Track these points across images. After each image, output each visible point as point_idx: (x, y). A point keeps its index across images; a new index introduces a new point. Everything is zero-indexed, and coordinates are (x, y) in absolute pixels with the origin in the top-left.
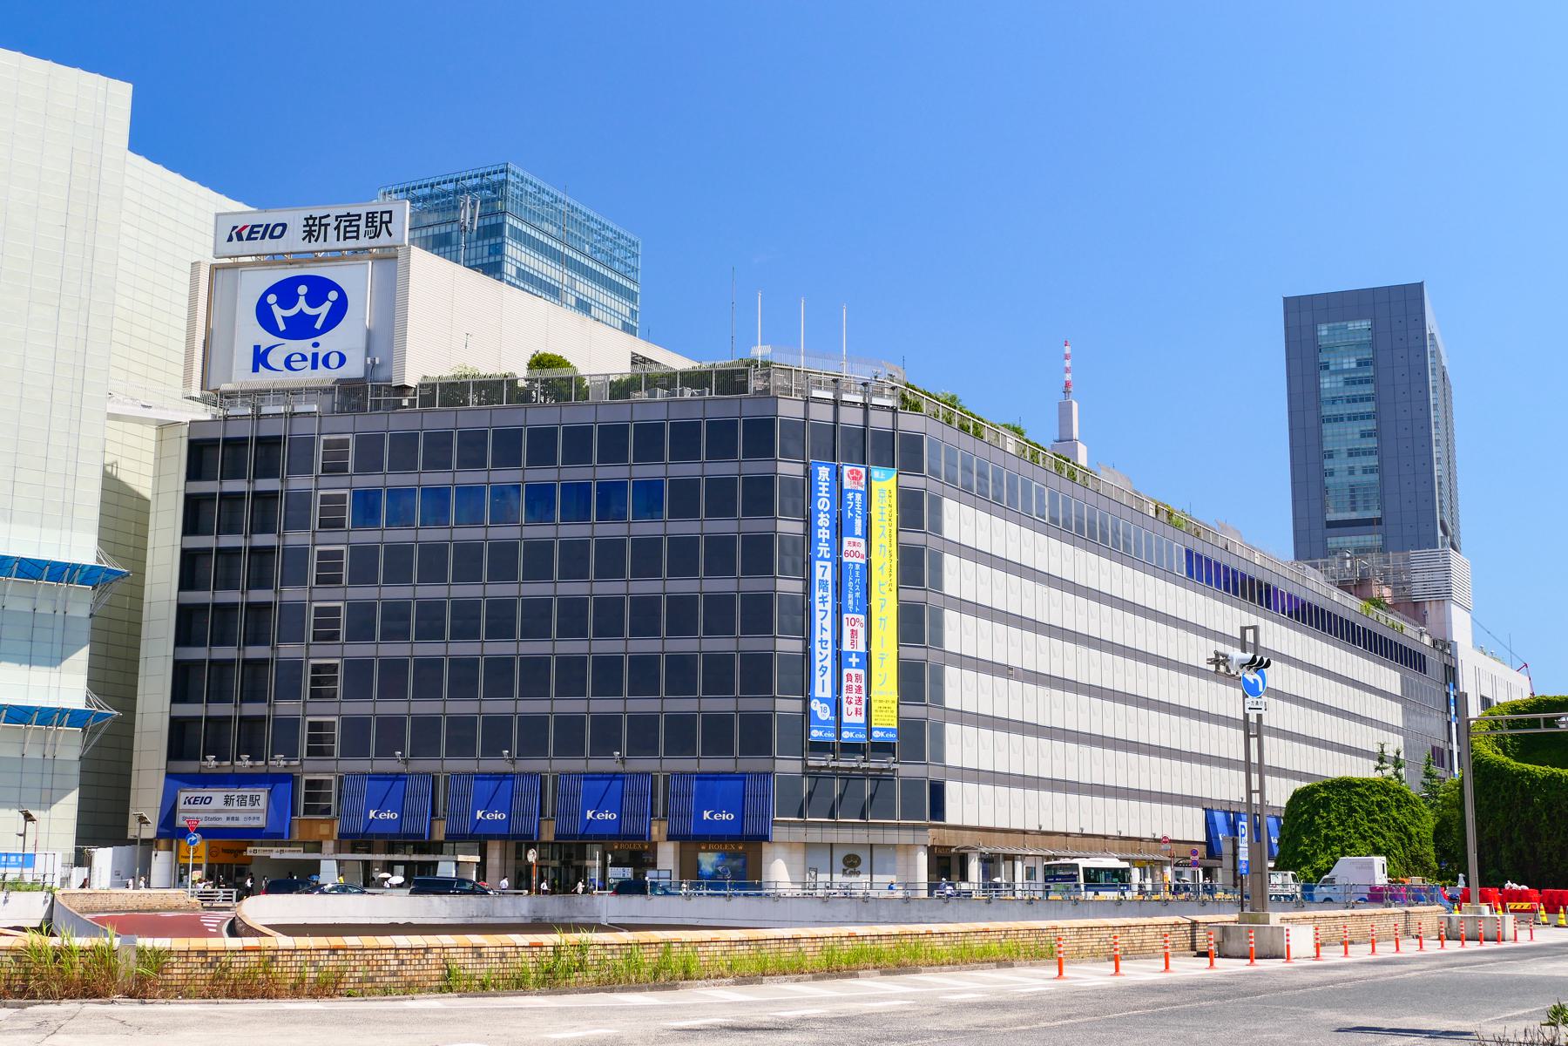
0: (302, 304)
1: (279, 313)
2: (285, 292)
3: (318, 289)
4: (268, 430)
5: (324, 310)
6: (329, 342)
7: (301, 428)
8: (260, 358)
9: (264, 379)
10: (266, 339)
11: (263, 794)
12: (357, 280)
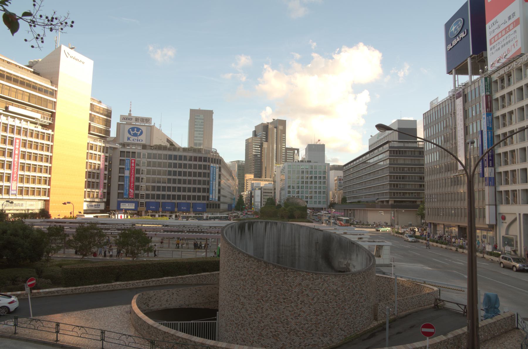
0: (135, 131)
1: (132, 132)
2: (133, 129)
3: (138, 129)
4: (133, 151)
5: (139, 133)
6: (140, 138)
7: (139, 151)
8: (129, 139)
9: (129, 141)
10: (130, 136)
11: (134, 204)
12: (144, 129)
